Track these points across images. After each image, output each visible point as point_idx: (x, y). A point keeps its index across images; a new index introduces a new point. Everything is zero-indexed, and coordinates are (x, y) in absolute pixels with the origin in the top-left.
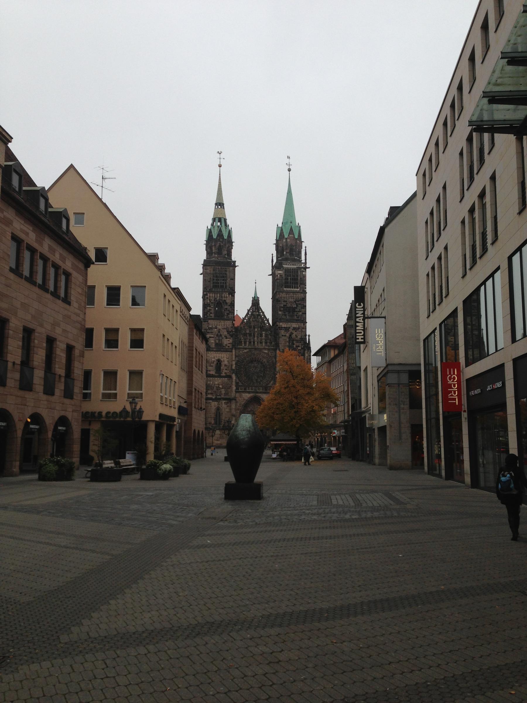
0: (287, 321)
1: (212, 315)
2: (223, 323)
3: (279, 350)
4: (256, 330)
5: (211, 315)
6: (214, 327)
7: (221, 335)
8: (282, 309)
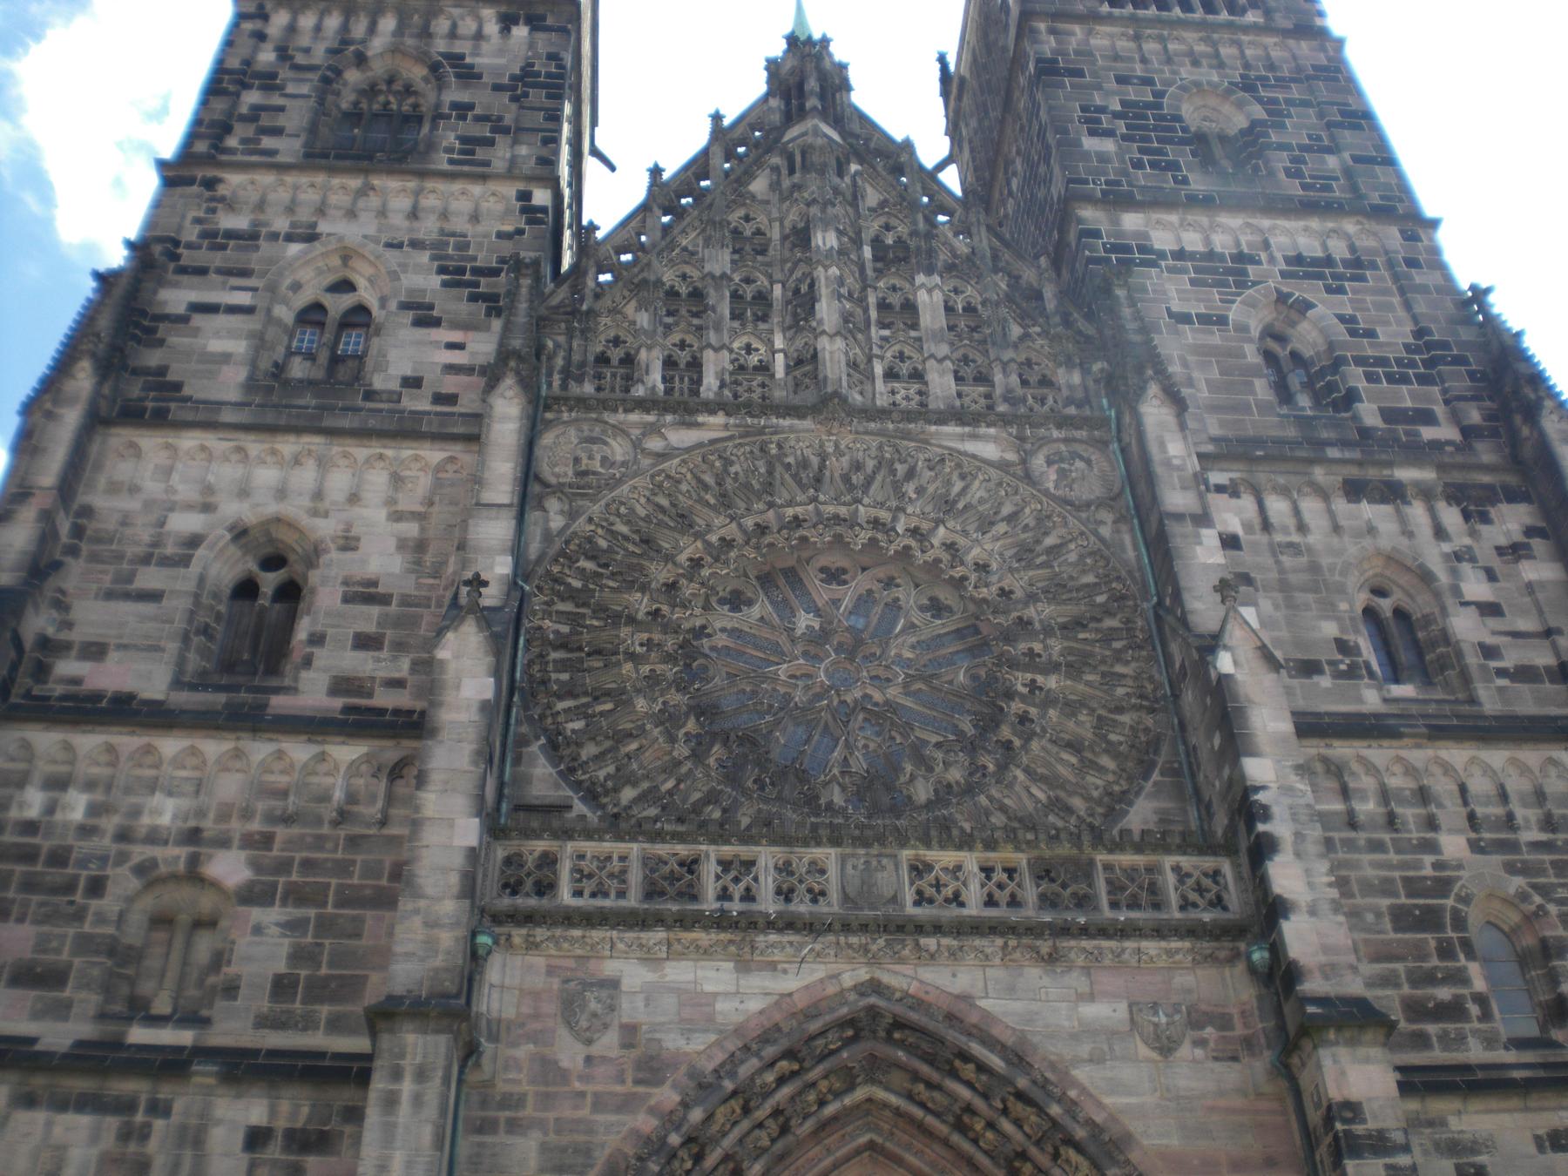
0: (1206, 203)
1: (288, 148)
2: (401, 204)
3: (1178, 402)
4: (825, 240)
5: (267, 142)
6: (281, 224)
7: (359, 317)
8: (1121, 126)
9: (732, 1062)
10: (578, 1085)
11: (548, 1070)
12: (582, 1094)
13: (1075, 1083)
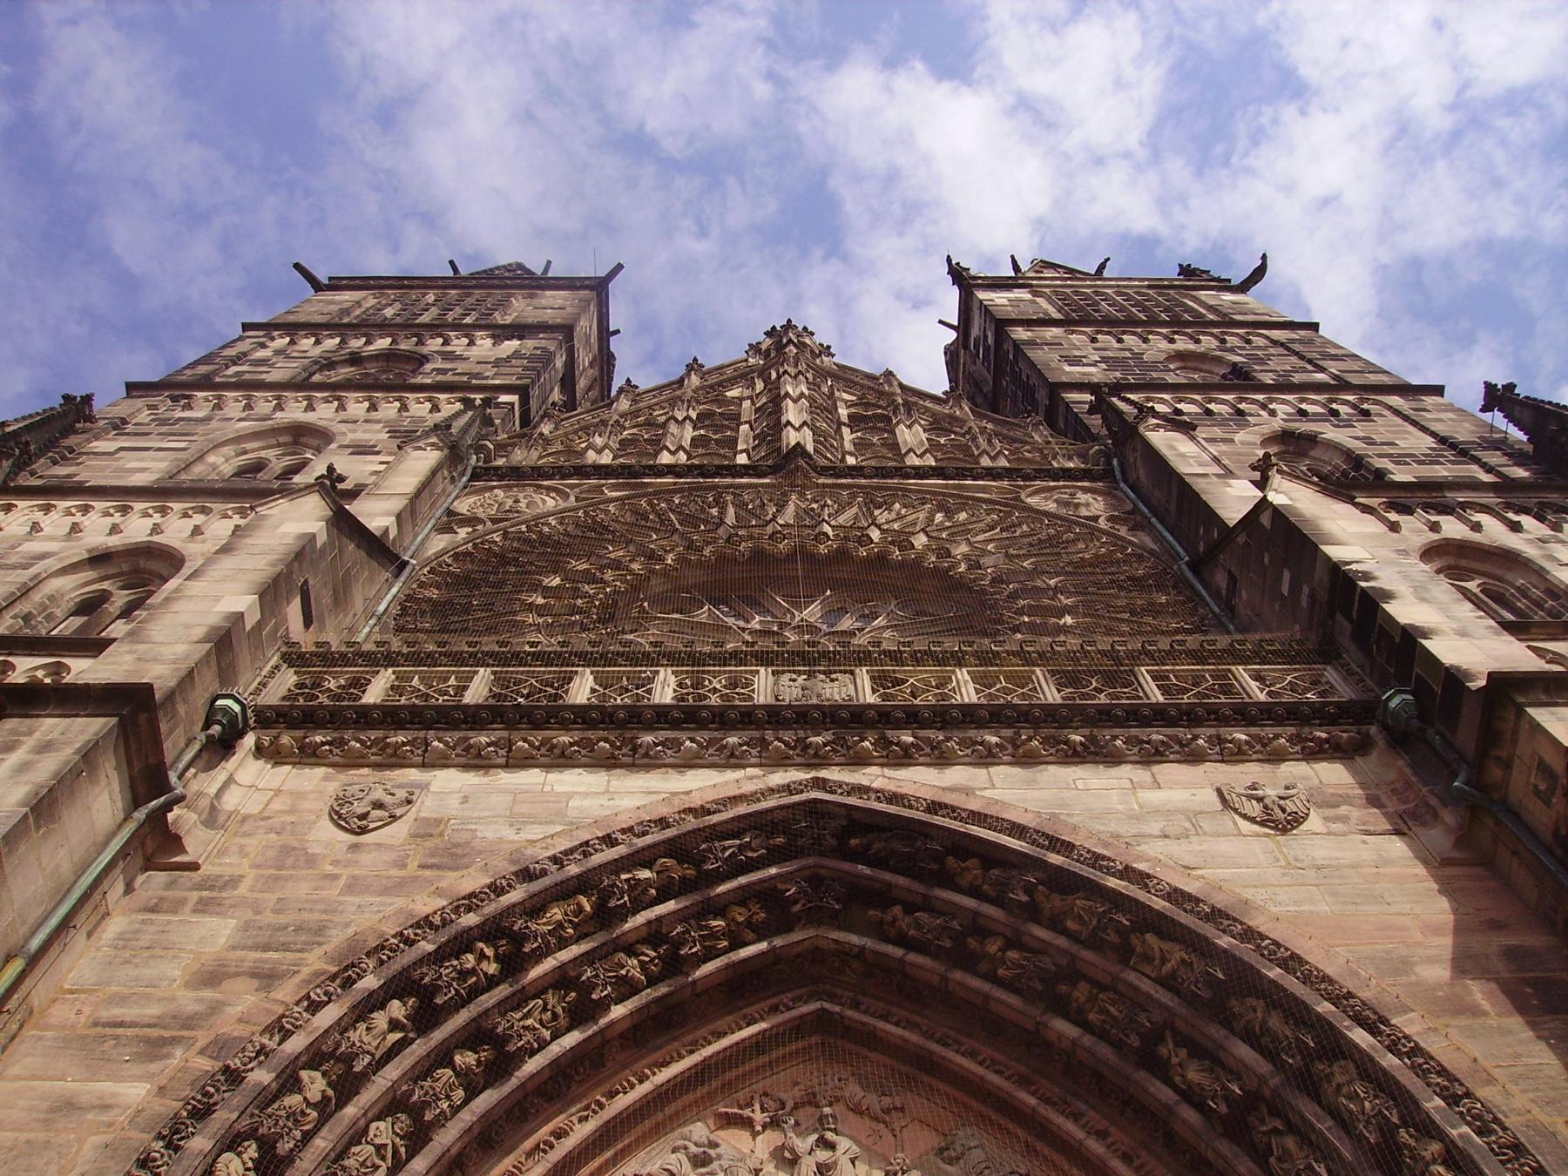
9: (585, 848)
10: (329, 869)
11: (290, 857)
12: (335, 877)
13: (1140, 858)
